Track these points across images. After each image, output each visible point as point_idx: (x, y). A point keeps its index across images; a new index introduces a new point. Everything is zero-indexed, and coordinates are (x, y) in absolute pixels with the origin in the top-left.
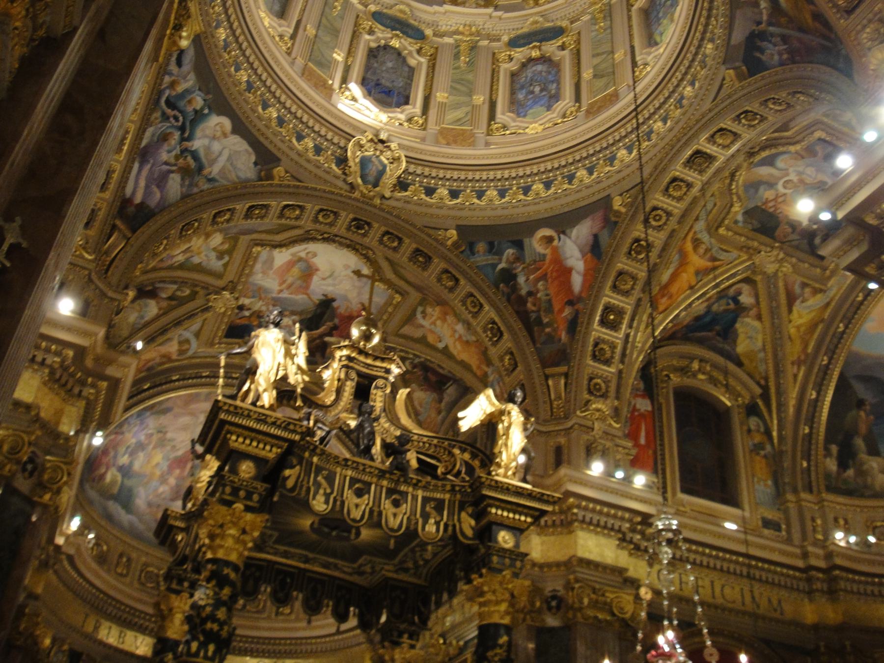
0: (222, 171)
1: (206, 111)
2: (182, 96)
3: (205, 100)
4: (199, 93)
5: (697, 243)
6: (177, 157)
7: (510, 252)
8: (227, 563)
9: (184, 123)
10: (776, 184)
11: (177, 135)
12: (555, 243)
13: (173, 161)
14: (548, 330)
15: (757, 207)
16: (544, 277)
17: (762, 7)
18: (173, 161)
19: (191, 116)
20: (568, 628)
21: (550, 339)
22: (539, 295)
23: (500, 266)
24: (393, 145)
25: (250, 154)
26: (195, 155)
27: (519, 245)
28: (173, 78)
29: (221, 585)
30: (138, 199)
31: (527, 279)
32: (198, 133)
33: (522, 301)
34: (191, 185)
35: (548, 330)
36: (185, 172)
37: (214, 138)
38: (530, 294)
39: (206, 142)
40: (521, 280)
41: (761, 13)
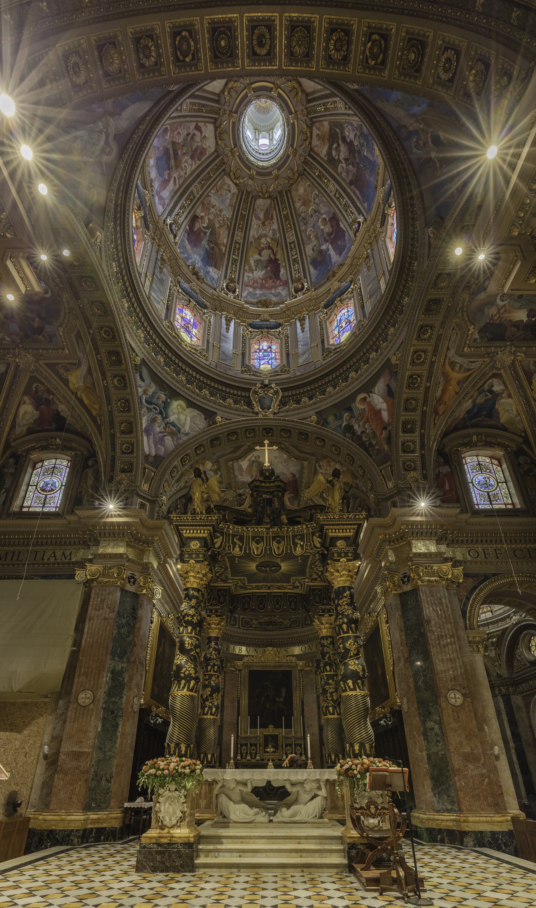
5: (453, 364)
6: (164, 428)
9: (160, 410)
10: (496, 301)
11: (160, 417)
12: (368, 399)
13: (163, 430)
15: (487, 324)
16: (367, 421)
18: (163, 430)
19: (162, 405)
23: (343, 425)
25: (200, 415)
26: (173, 424)
27: (350, 409)
32: (170, 413)
33: (360, 438)
36: (172, 434)
37: (179, 413)
38: (363, 432)
39: (176, 416)
40: (356, 427)
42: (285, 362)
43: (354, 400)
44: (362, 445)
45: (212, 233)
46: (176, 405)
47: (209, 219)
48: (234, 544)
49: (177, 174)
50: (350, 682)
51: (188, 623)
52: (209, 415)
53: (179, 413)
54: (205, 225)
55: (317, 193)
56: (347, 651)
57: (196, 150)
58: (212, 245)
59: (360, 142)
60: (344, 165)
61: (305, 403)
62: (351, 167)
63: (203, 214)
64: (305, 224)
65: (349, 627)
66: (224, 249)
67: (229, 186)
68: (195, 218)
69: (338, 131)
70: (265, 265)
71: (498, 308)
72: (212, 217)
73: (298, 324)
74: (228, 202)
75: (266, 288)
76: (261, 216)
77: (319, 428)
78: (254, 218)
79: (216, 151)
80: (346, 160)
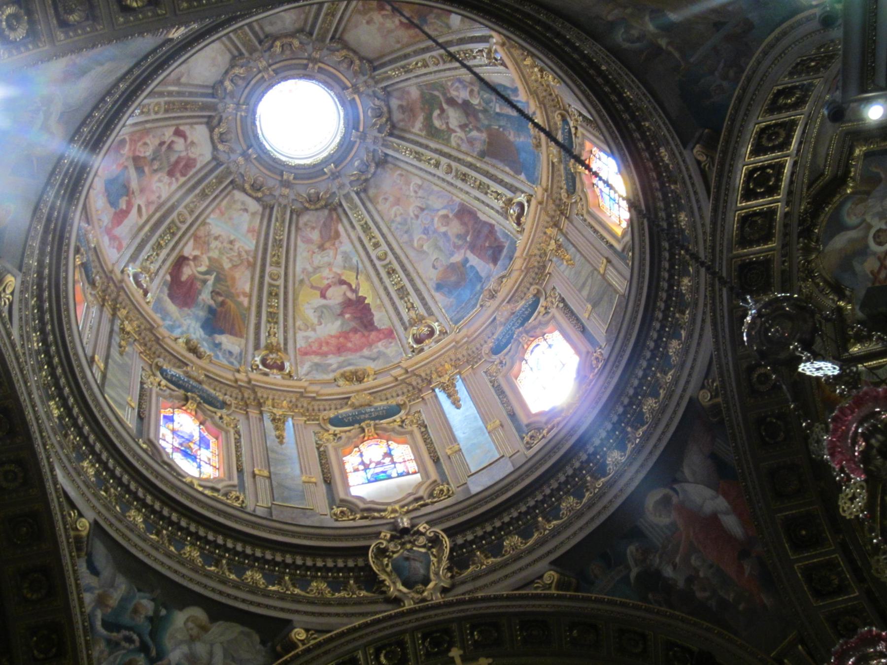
1: (163, 612)
3: (153, 600)
4: (142, 594)
9: (142, 642)
10: (867, 246)
12: (675, 500)
14: (741, 607)
15: (870, 291)
17: (664, 47)
19: (147, 627)
22: (701, 574)
23: (633, 575)
27: (636, 534)
28: (97, 592)
31: (675, 567)
32: (168, 643)
35: (741, 607)
37: (192, 639)
38: (690, 580)
39: (185, 649)
40: (668, 572)
41: (670, 53)
42: (434, 475)
45: (218, 280)
47: (210, 259)
49: (144, 199)
53: (192, 639)
54: (203, 269)
55: (420, 182)
57: (177, 162)
58: (220, 299)
59: (482, 98)
60: (460, 133)
61: (514, 548)
62: (474, 133)
63: (197, 253)
64: (406, 232)
66: (245, 301)
67: (243, 203)
68: (181, 261)
69: (436, 93)
70: (339, 311)
71: (879, 258)
72: (215, 254)
73: (442, 396)
74: (245, 227)
75: (350, 350)
76: (315, 236)
77: (571, 598)
78: (299, 243)
79: (214, 158)
80: (463, 127)
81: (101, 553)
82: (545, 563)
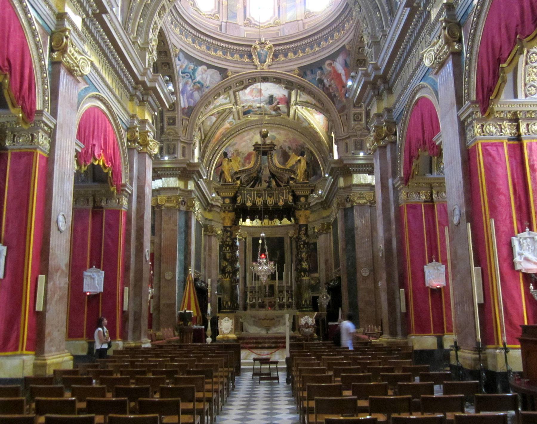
0: (210, 82)
2: (186, 68)
6: (193, 87)
7: (319, 72)
8: (227, 227)
11: (190, 80)
16: (332, 79)
20: (352, 207)
21: (340, 101)
23: (317, 78)
24: (268, 42)
26: (199, 83)
27: (321, 68)
29: (227, 232)
30: (187, 106)
32: (196, 75)
33: (328, 89)
34: (201, 93)
36: (198, 89)
37: (203, 73)
38: (330, 86)
39: (200, 76)
40: (325, 81)
43: (324, 63)
44: (330, 95)
46: (201, 69)
48: (247, 199)
50: (303, 274)
51: (227, 245)
52: (223, 72)
53: (203, 73)
56: (302, 258)
65: (304, 246)
77: (300, 79)
81: (181, 56)
82: (296, 67)
